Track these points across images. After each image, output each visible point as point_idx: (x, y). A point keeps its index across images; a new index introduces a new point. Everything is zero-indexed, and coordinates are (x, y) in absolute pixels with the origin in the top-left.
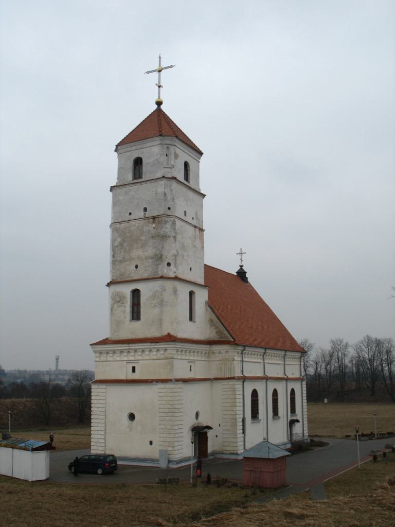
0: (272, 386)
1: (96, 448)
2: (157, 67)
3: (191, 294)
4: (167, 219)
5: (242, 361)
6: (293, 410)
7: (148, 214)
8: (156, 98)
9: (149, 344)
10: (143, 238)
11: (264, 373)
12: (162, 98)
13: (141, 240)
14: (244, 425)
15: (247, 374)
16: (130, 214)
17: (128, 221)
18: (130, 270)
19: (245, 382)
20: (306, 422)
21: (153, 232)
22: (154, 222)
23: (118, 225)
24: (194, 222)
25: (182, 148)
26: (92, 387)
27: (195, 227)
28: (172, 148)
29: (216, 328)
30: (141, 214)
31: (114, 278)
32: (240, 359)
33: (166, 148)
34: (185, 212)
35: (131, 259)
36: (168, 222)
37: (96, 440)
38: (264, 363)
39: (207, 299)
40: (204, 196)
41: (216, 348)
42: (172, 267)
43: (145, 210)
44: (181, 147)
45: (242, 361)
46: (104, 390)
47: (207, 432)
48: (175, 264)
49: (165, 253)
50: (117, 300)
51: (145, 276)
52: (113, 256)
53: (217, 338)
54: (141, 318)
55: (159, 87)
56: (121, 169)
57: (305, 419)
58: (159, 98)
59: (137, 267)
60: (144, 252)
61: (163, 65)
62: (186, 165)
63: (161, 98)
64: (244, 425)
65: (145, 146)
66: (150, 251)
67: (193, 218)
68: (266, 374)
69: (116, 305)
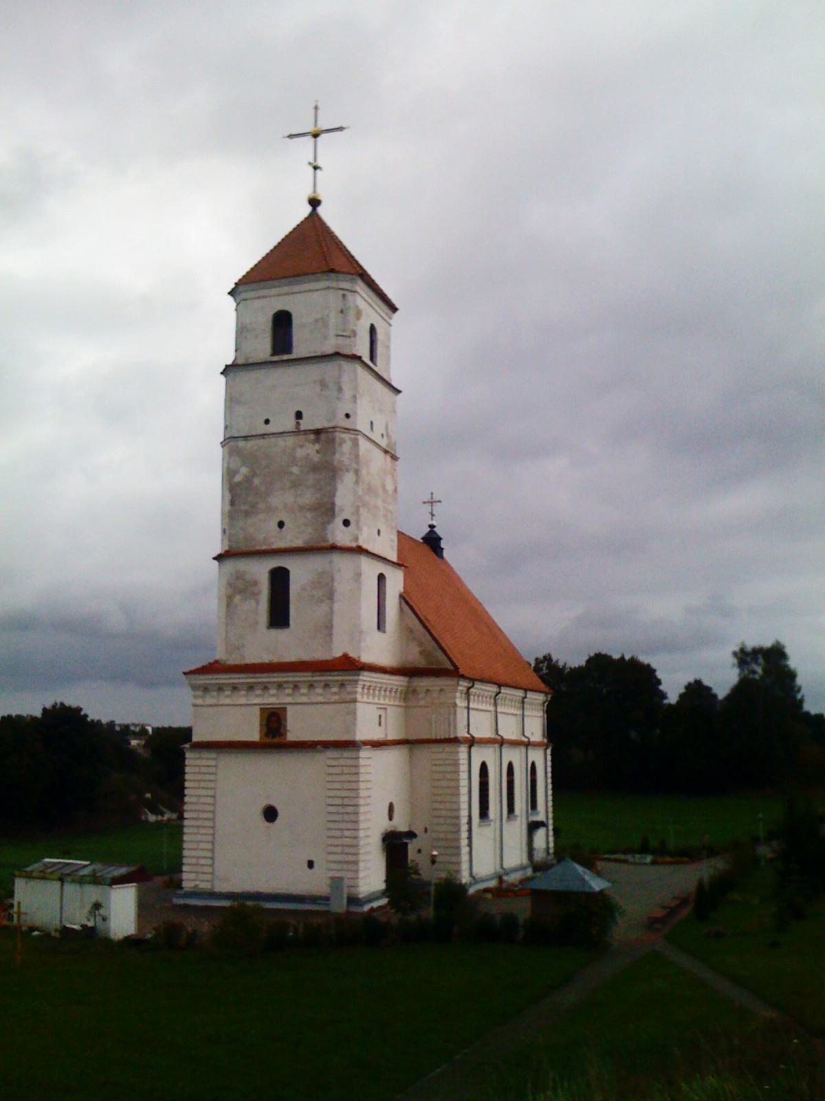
0: (510, 755)
1: (192, 876)
2: (310, 128)
3: (381, 577)
6: (534, 805)
7: (305, 424)
8: (308, 193)
9: (310, 674)
10: (295, 470)
11: (497, 730)
12: (322, 196)
13: (291, 473)
14: (470, 830)
16: (267, 422)
17: (263, 436)
18: (265, 532)
19: (503, 747)
20: (551, 828)
21: (316, 458)
22: (317, 441)
23: (241, 444)
24: (383, 443)
25: (367, 298)
26: (188, 755)
28: (350, 296)
29: (421, 644)
30: (290, 424)
31: (234, 545)
32: (464, 704)
33: (340, 296)
34: (372, 423)
35: (270, 510)
37: (193, 861)
38: (496, 712)
39: (402, 590)
40: (398, 392)
41: (423, 683)
43: (299, 415)
44: (364, 295)
45: (468, 708)
46: (212, 763)
47: (407, 844)
48: (357, 522)
49: (339, 501)
50: (237, 589)
51: (299, 543)
52: (232, 503)
53: (421, 662)
54: (291, 622)
55: (316, 168)
56: (242, 331)
57: (551, 821)
58: (315, 191)
59: (281, 525)
60: (296, 497)
61: (323, 125)
62: (373, 330)
63: (319, 190)
64: (470, 830)
65: (297, 288)
66: (308, 498)
67: (382, 435)
69: (237, 598)
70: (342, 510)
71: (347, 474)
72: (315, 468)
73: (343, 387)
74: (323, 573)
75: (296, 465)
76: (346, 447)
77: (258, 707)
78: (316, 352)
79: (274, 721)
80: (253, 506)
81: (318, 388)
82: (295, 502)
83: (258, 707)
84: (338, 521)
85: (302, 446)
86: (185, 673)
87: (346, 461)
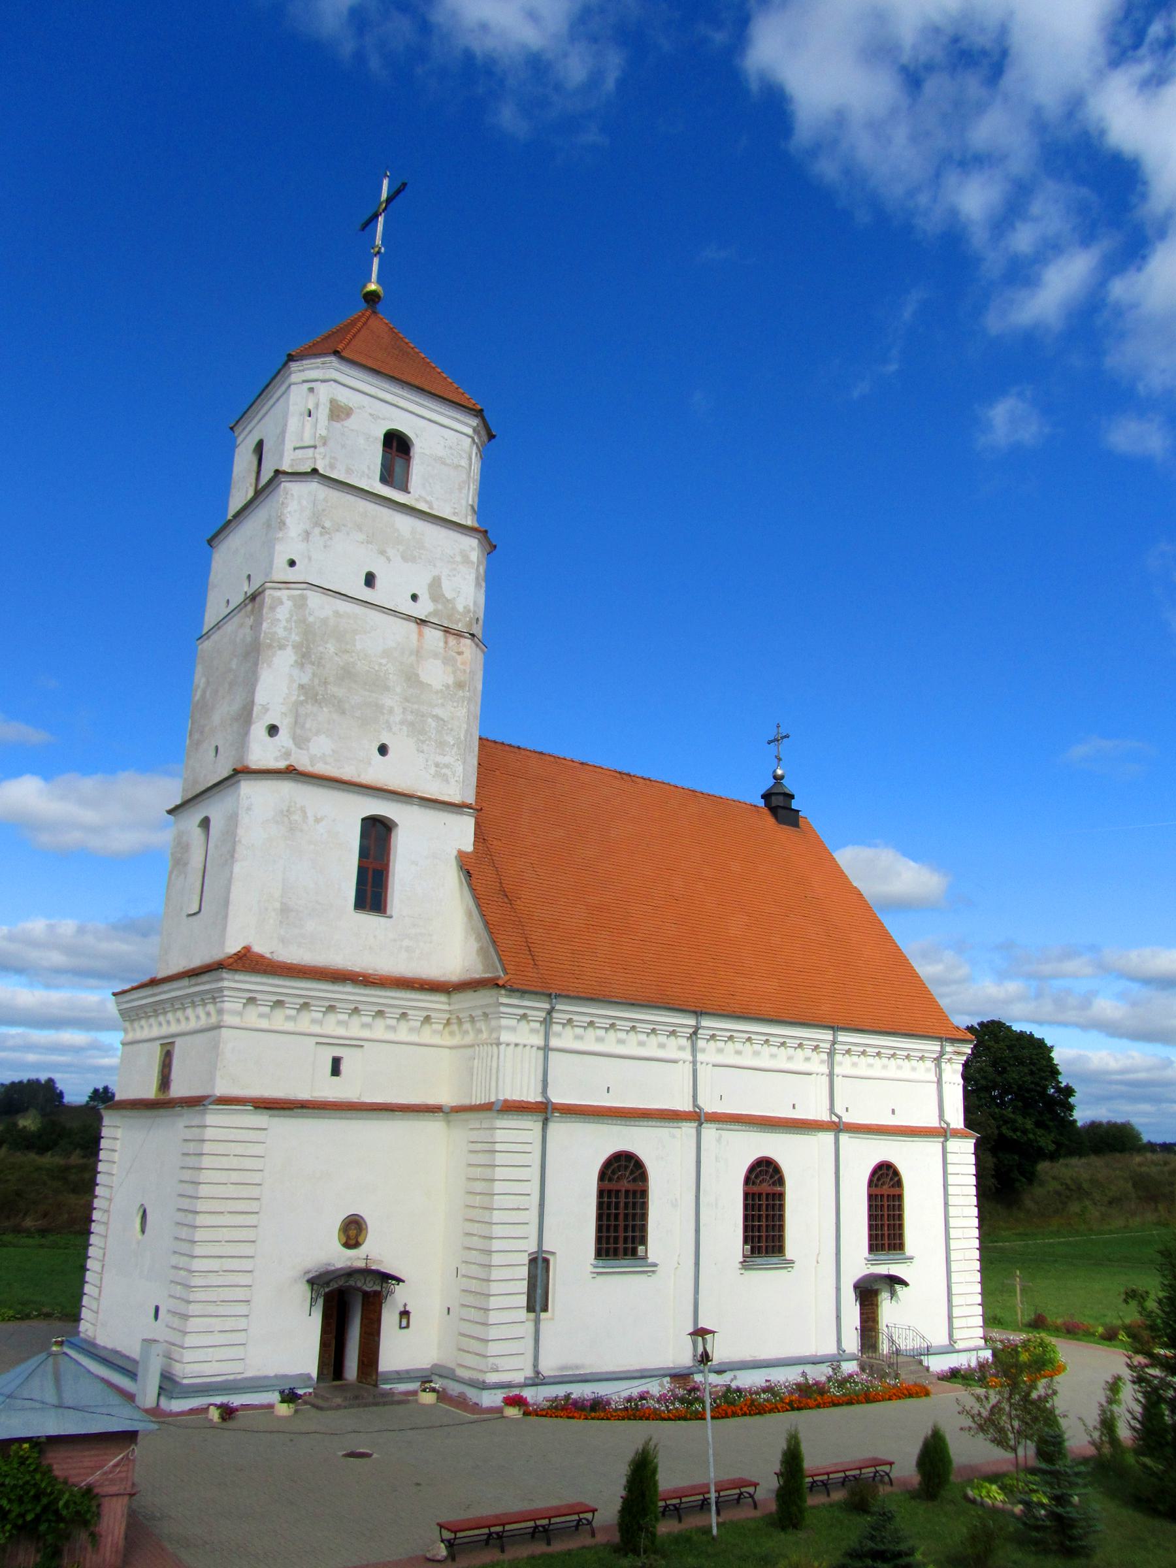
4: (278, 593)
5: (546, 1049)
15: (709, 1105)
25: (389, 397)
27: (422, 622)
36: (282, 603)
39: (469, 848)
42: (283, 736)
49: (262, 696)
67: (414, 597)
68: (700, 1102)
70: (266, 709)
71: (279, 652)
73: (288, 521)
76: (283, 612)
77: (159, 1042)
83: (159, 1042)
84: (258, 731)
86: (114, 994)
87: (281, 633)
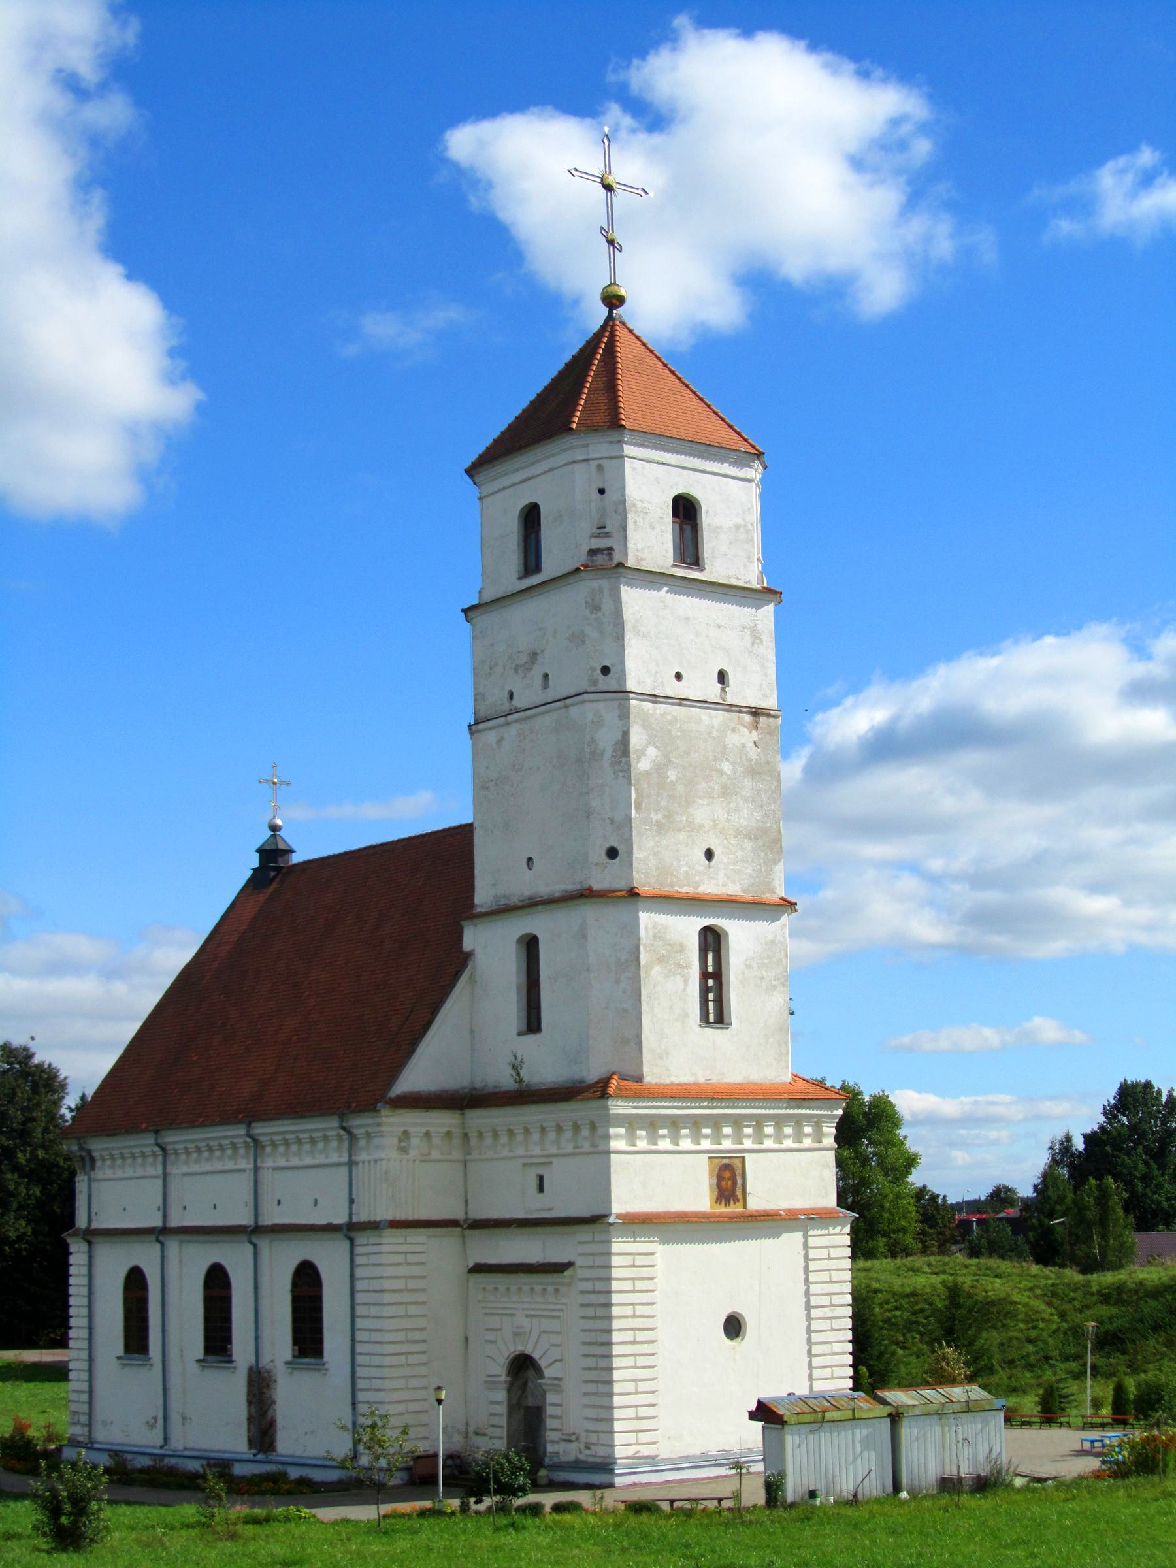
10: (727, 767)
30: (704, 686)
43: (722, 677)
51: (734, 889)
59: (709, 854)
72: (754, 771)
74: (773, 942)
75: (727, 760)
78: (738, 579)
79: (729, 1181)
80: (669, 816)
81: (748, 639)
82: (728, 820)
85: (733, 730)
